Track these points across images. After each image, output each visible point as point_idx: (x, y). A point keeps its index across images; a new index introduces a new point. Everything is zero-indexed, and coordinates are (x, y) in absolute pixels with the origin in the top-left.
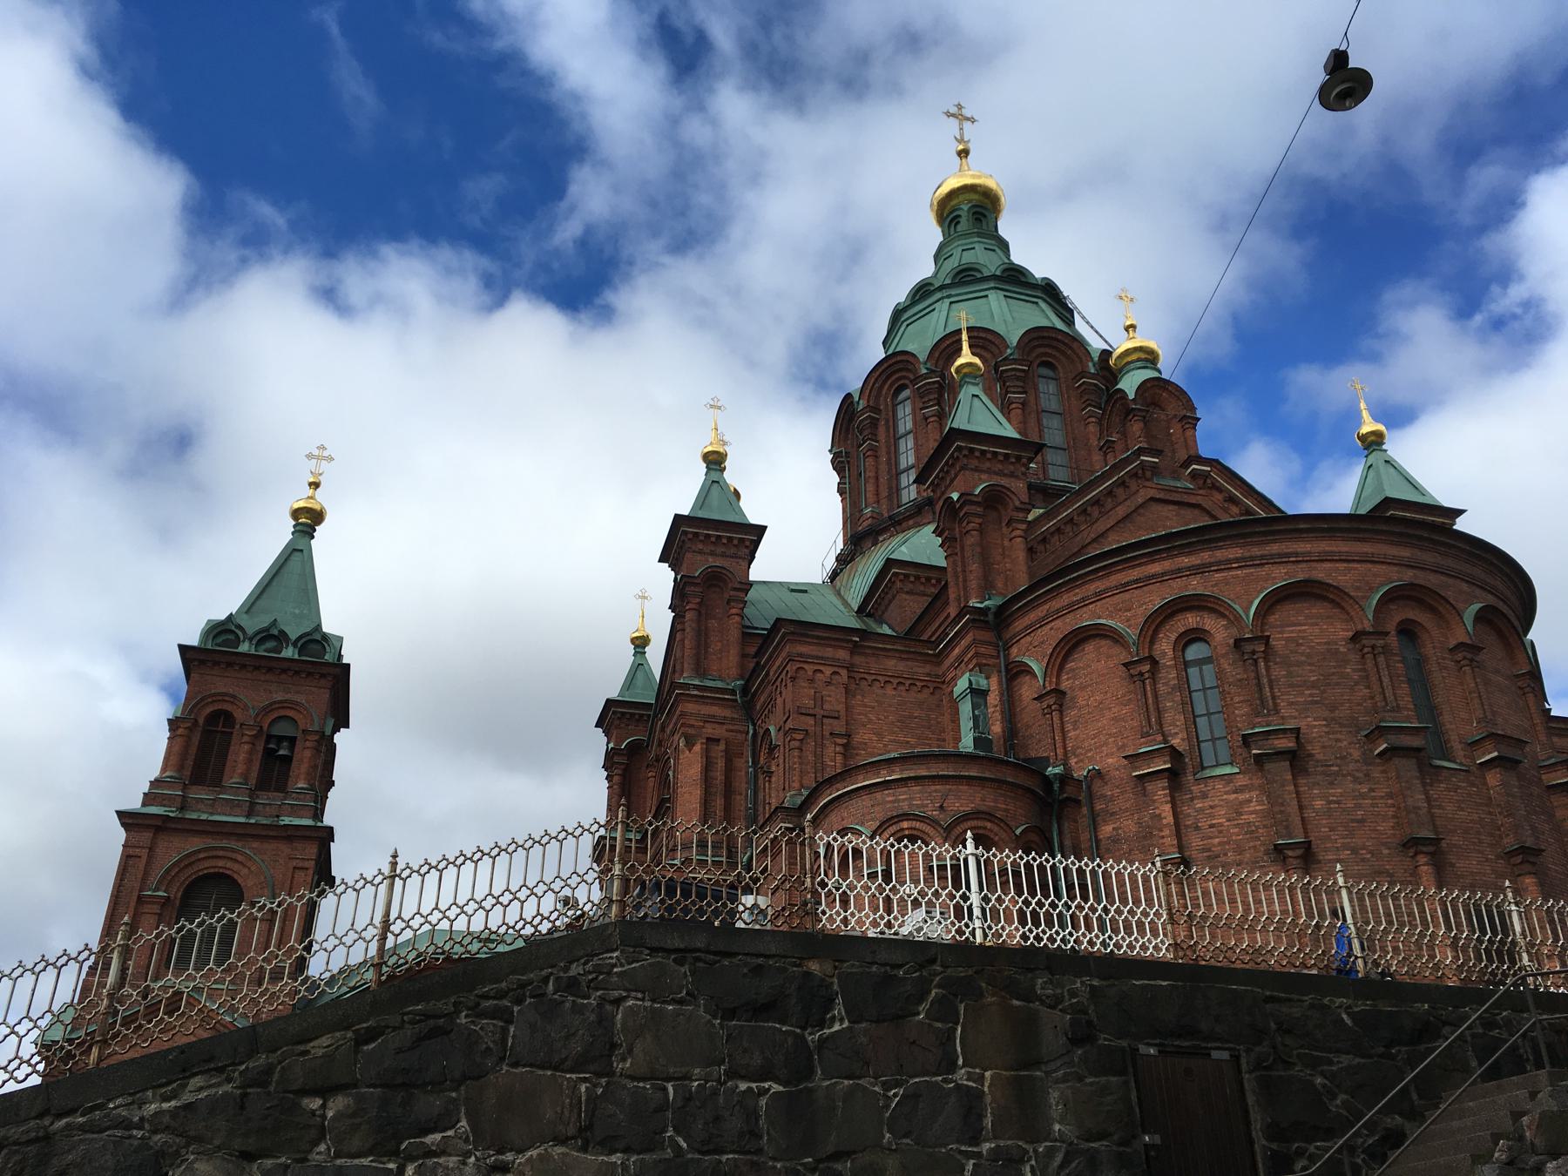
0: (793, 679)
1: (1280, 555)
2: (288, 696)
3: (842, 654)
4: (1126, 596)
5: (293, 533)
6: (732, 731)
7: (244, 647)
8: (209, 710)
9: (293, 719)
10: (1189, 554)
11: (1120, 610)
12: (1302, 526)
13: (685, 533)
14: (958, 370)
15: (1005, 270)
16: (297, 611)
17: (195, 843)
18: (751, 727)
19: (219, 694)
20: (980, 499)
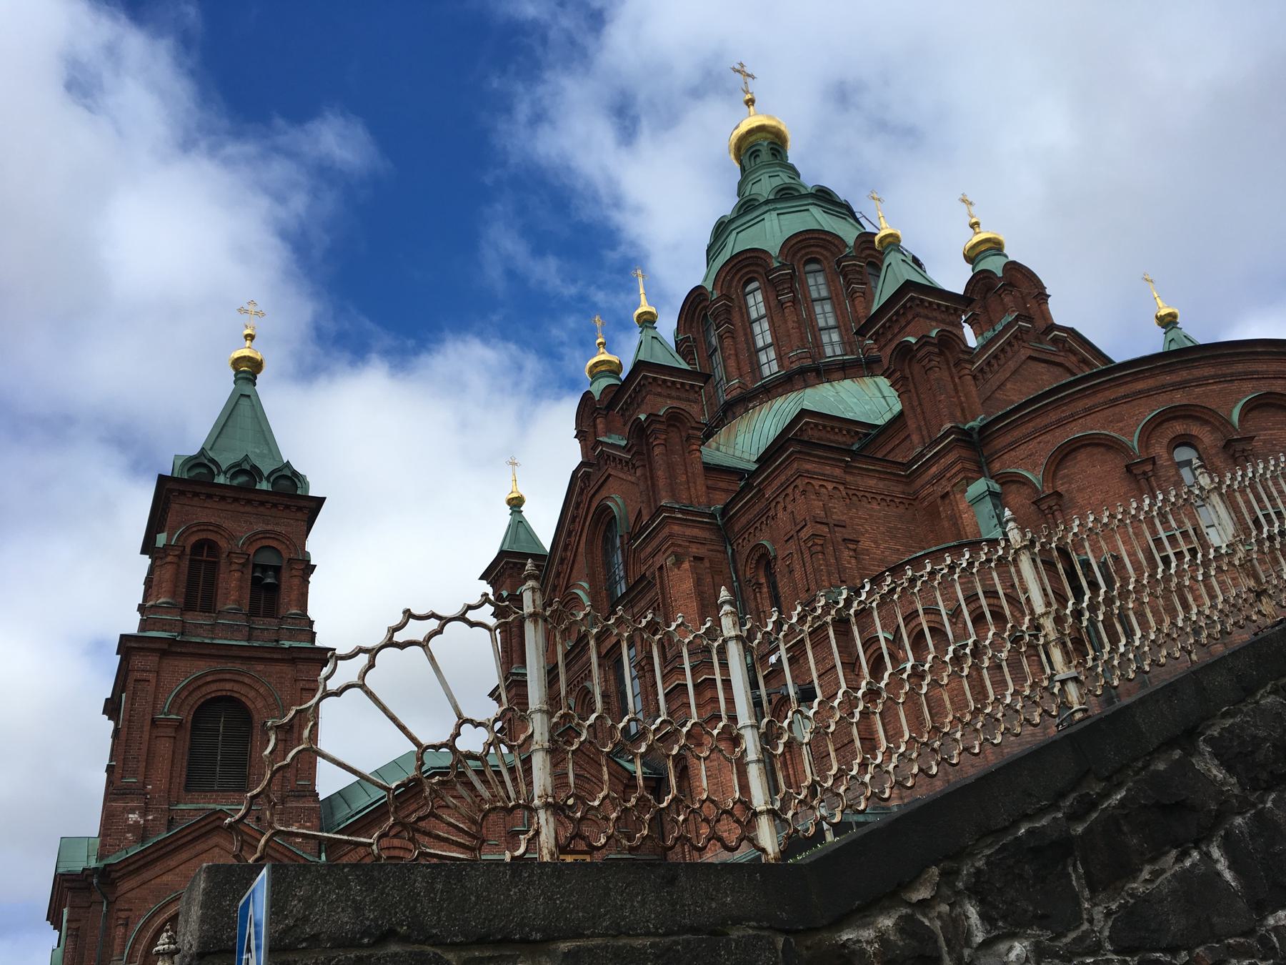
0: (804, 492)
1: (1246, 373)
2: (269, 528)
3: (837, 472)
4: (1117, 410)
5: (235, 383)
6: (712, 551)
7: (221, 480)
8: (194, 539)
9: (273, 547)
10: (1171, 372)
11: (1111, 422)
12: (1259, 350)
13: (645, 377)
14: (881, 240)
15: (817, 191)
16: (258, 451)
17: (200, 668)
18: (729, 547)
19: (204, 524)
20: (936, 341)
